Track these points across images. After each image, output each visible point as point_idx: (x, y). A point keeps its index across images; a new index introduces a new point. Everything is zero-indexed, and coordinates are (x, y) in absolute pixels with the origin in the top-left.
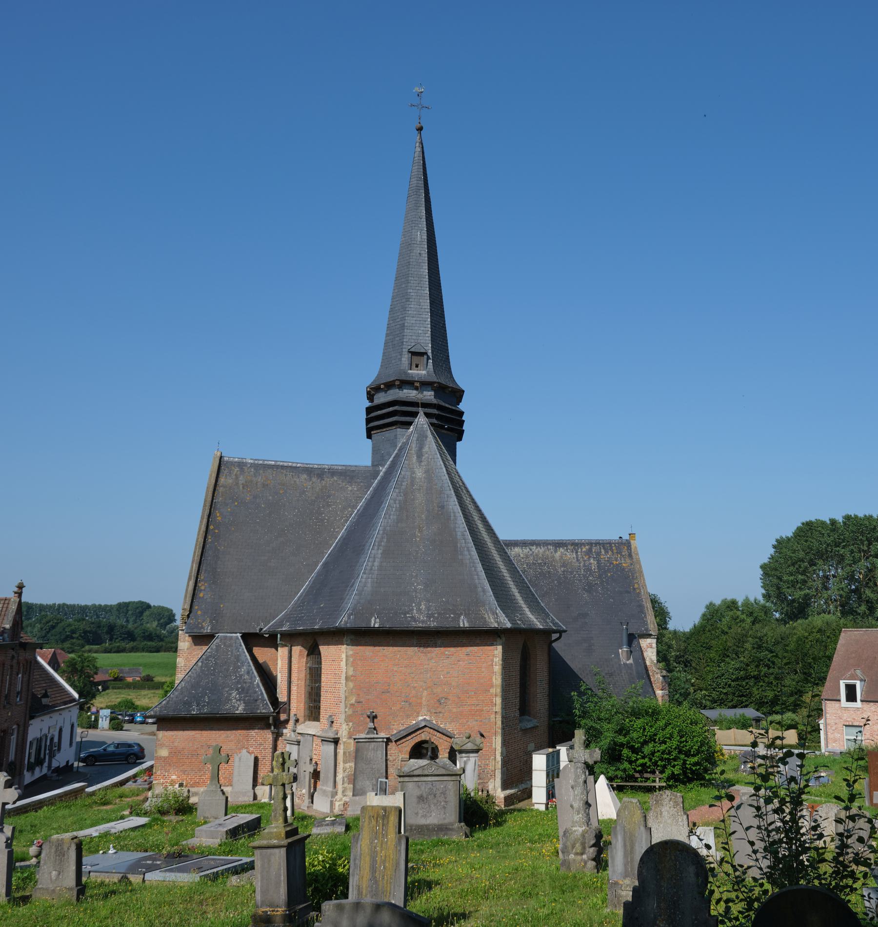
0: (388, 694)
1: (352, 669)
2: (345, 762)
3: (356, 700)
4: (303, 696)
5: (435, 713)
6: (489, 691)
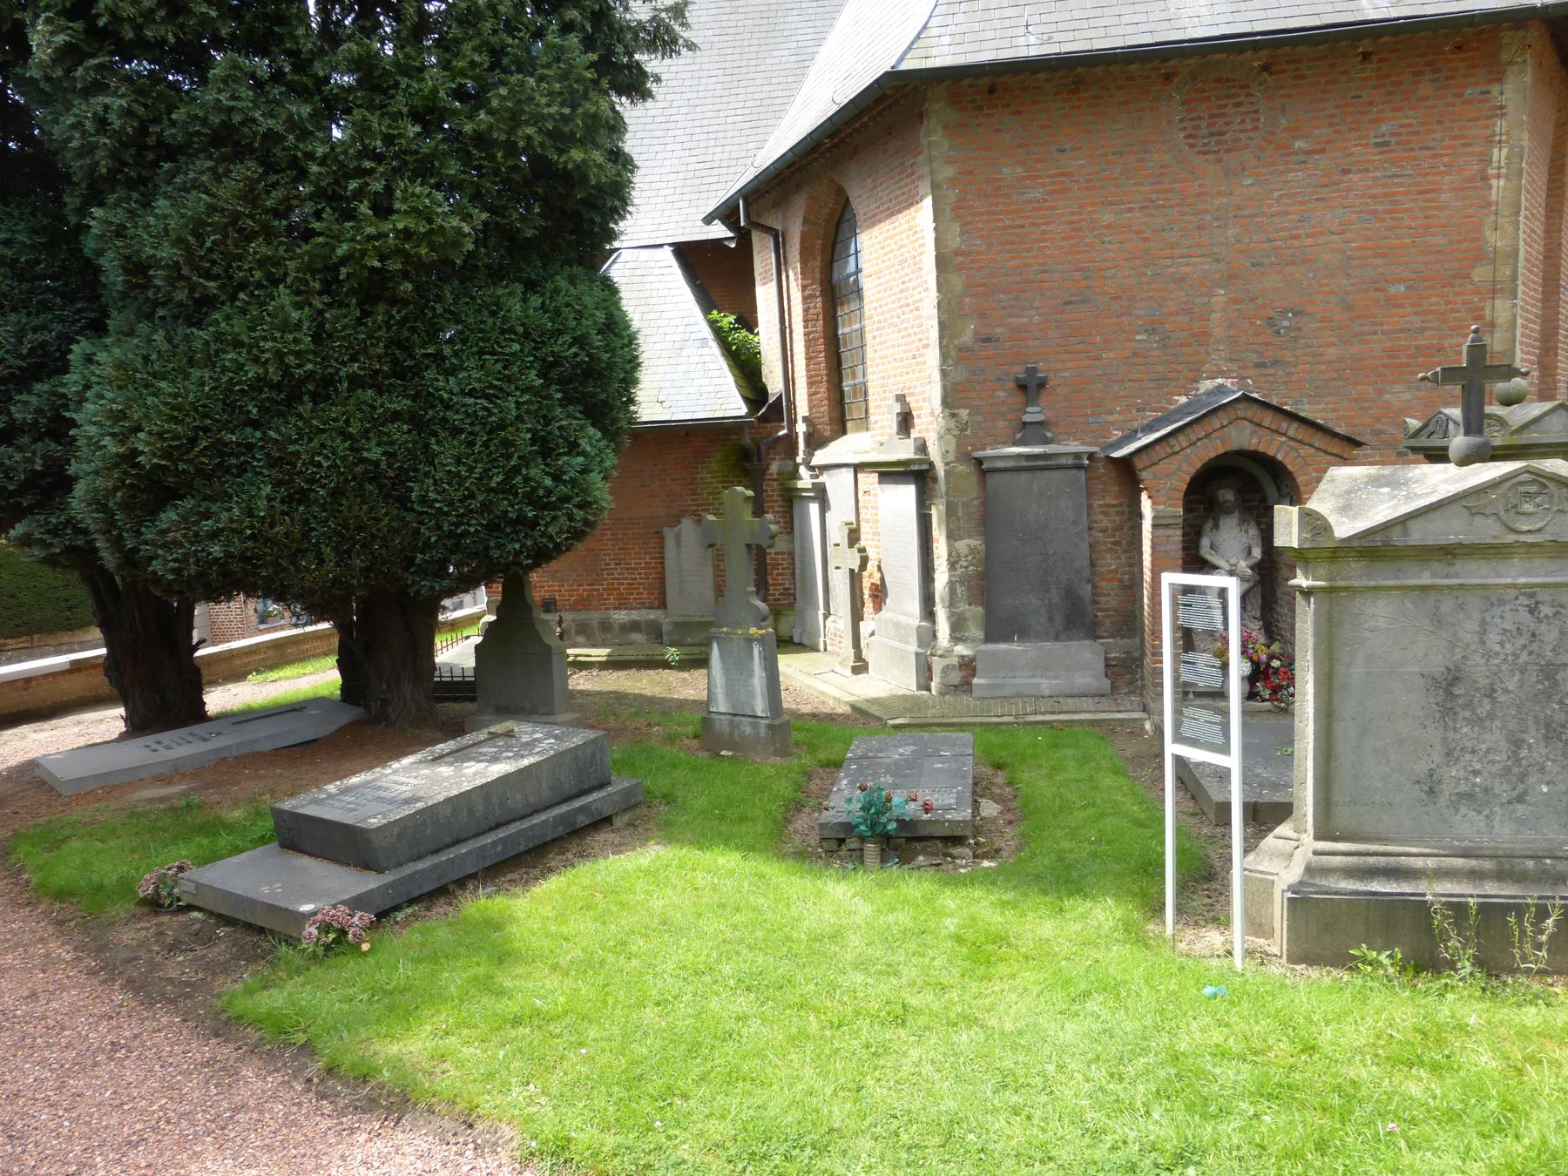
1: (956, 227)
2: (951, 537)
3: (976, 333)
5: (1257, 365)
6: (1467, 276)
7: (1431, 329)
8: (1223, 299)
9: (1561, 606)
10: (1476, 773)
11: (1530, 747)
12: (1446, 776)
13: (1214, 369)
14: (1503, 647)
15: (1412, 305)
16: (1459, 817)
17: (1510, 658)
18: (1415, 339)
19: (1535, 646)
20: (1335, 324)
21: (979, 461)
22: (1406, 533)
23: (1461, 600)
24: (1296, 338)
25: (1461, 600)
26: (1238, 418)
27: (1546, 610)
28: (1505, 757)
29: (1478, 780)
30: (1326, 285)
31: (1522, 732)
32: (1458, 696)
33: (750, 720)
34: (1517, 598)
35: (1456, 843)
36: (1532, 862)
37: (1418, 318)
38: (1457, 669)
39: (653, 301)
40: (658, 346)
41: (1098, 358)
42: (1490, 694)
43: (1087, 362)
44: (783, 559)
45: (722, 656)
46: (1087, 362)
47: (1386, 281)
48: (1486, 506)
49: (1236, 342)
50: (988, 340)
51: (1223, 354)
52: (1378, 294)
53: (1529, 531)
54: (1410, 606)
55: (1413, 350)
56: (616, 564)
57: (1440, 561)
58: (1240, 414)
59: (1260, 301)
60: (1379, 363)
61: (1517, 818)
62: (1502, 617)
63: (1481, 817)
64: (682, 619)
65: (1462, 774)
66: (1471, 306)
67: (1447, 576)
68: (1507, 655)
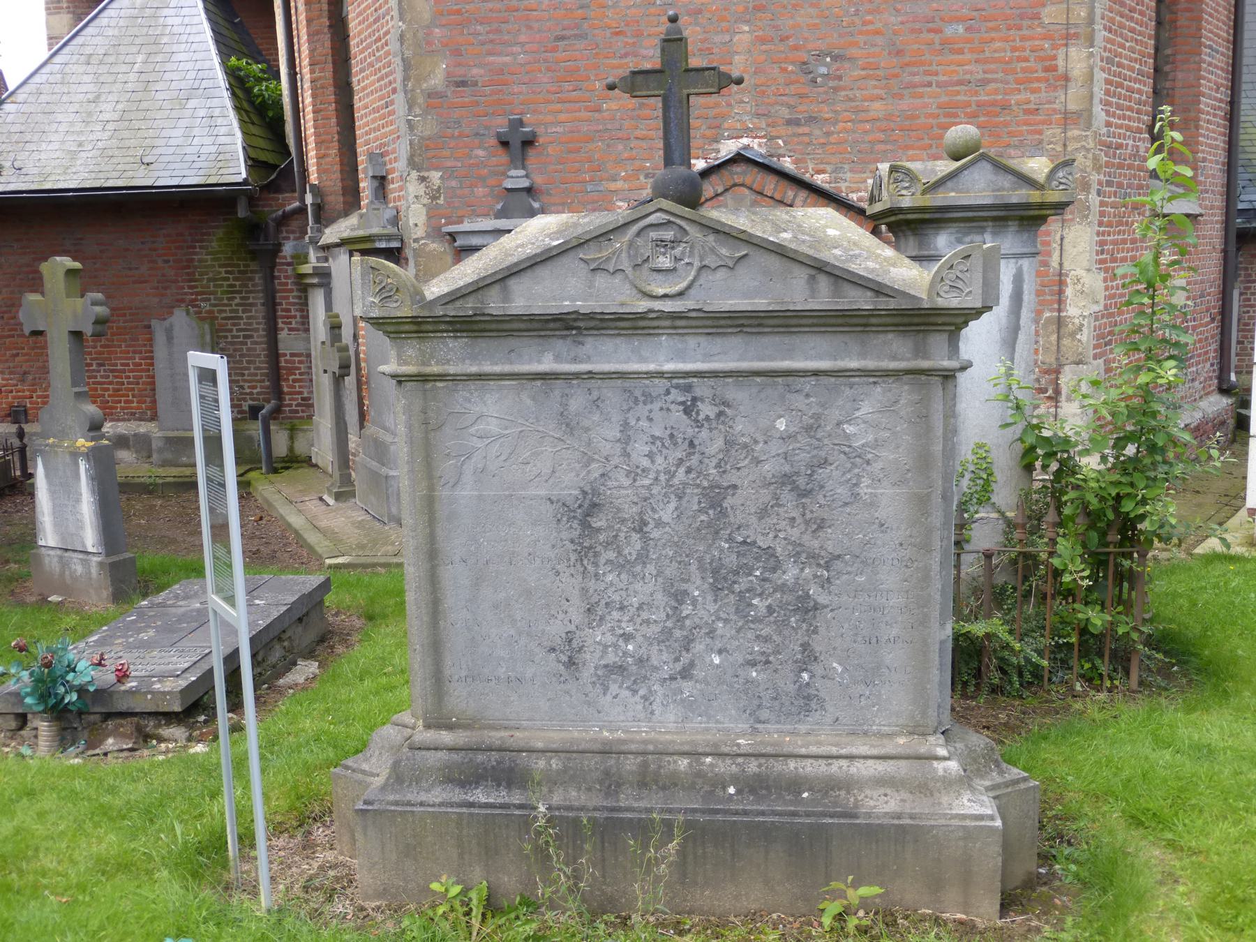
0: (580, 44)
3: (449, 74)
4: (334, 120)
5: (789, 122)
6: (1037, 17)
7: (995, 81)
8: (747, 37)
9: (726, 404)
10: (627, 637)
11: (694, 602)
12: (589, 641)
13: (738, 126)
14: (653, 462)
15: (972, 51)
16: (609, 698)
17: (662, 477)
18: (976, 93)
19: (694, 460)
20: (881, 73)
21: (453, 236)
22: (506, 298)
23: (595, 394)
24: (836, 89)
25: (595, 394)
26: (735, 185)
27: (707, 410)
28: (663, 616)
29: (630, 647)
30: (872, 22)
31: (683, 580)
32: (598, 530)
33: (81, 556)
34: (668, 393)
35: (606, 734)
36: (686, 762)
37: (980, 68)
38: (595, 492)
39: (165, 40)
40: (160, 96)
41: (599, 110)
42: (640, 527)
43: (584, 114)
44: (300, 362)
45: (47, 476)
46: (584, 114)
47: (942, 19)
48: (608, 259)
49: (764, 92)
50: (463, 84)
51: (748, 109)
52: (931, 36)
53: (665, 296)
54: (529, 402)
55: (974, 107)
56: (100, 365)
57: (564, 337)
58: (737, 179)
59: (791, 42)
60: (934, 122)
61: (683, 700)
62: (650, 420)
63: (637, 698)
64: (176, 434)
65: (609, 639)
66: (1042, 54)
67: (575, 360)
68: (658, 472)
